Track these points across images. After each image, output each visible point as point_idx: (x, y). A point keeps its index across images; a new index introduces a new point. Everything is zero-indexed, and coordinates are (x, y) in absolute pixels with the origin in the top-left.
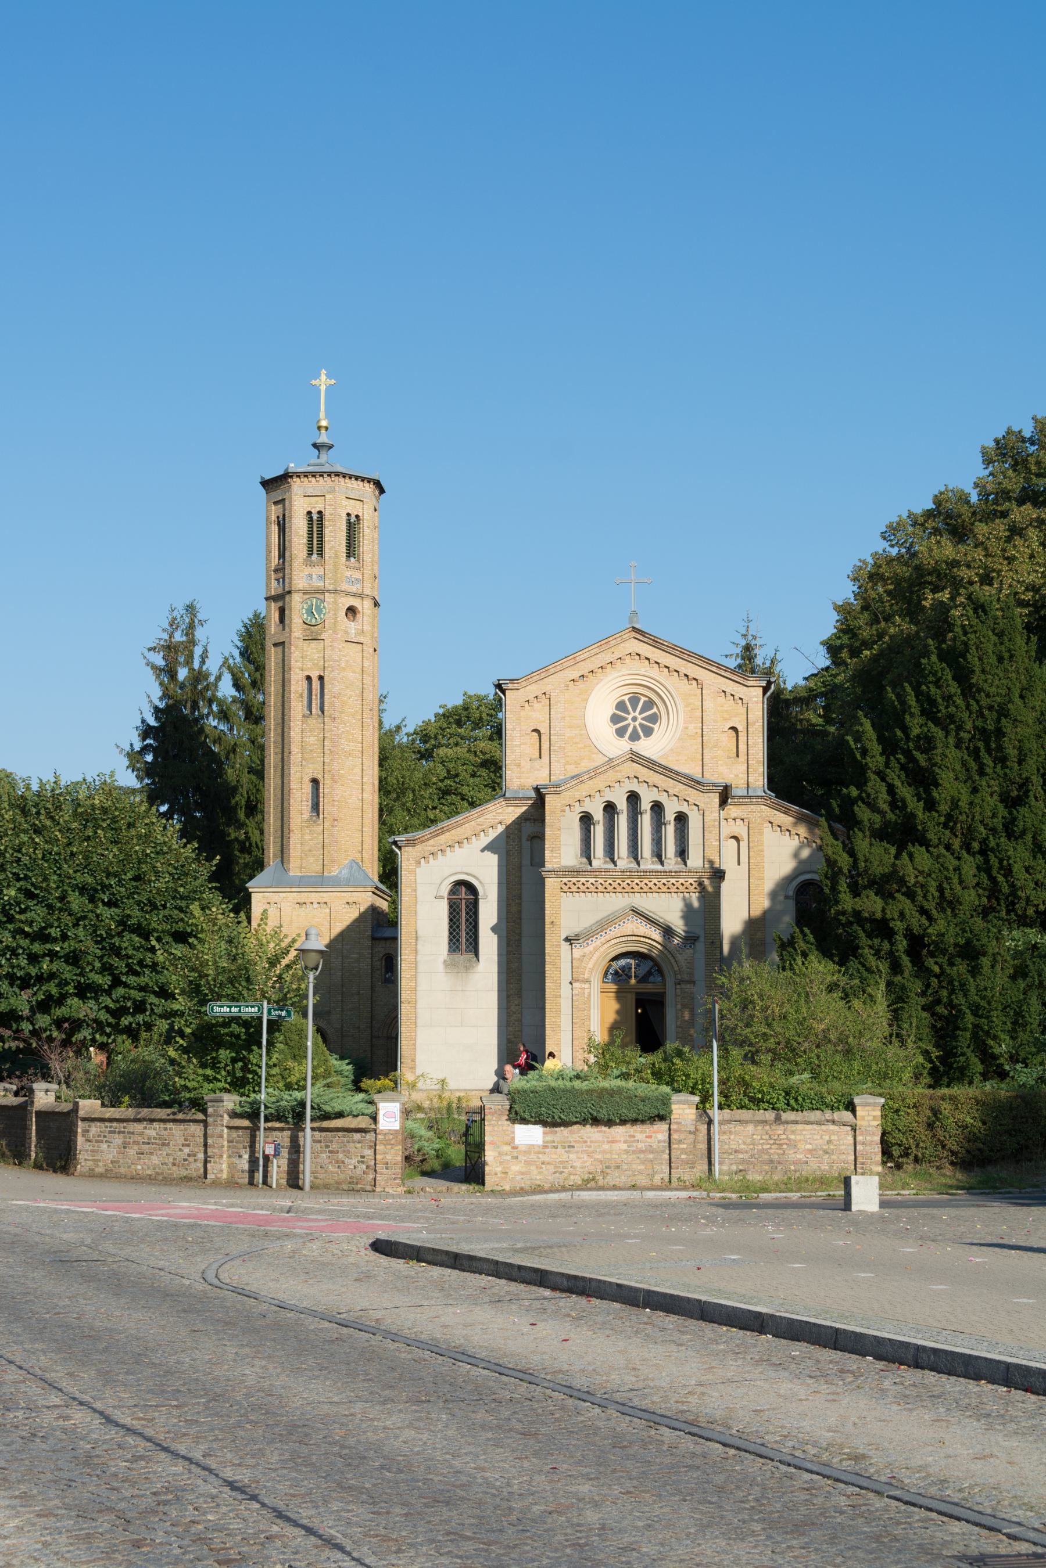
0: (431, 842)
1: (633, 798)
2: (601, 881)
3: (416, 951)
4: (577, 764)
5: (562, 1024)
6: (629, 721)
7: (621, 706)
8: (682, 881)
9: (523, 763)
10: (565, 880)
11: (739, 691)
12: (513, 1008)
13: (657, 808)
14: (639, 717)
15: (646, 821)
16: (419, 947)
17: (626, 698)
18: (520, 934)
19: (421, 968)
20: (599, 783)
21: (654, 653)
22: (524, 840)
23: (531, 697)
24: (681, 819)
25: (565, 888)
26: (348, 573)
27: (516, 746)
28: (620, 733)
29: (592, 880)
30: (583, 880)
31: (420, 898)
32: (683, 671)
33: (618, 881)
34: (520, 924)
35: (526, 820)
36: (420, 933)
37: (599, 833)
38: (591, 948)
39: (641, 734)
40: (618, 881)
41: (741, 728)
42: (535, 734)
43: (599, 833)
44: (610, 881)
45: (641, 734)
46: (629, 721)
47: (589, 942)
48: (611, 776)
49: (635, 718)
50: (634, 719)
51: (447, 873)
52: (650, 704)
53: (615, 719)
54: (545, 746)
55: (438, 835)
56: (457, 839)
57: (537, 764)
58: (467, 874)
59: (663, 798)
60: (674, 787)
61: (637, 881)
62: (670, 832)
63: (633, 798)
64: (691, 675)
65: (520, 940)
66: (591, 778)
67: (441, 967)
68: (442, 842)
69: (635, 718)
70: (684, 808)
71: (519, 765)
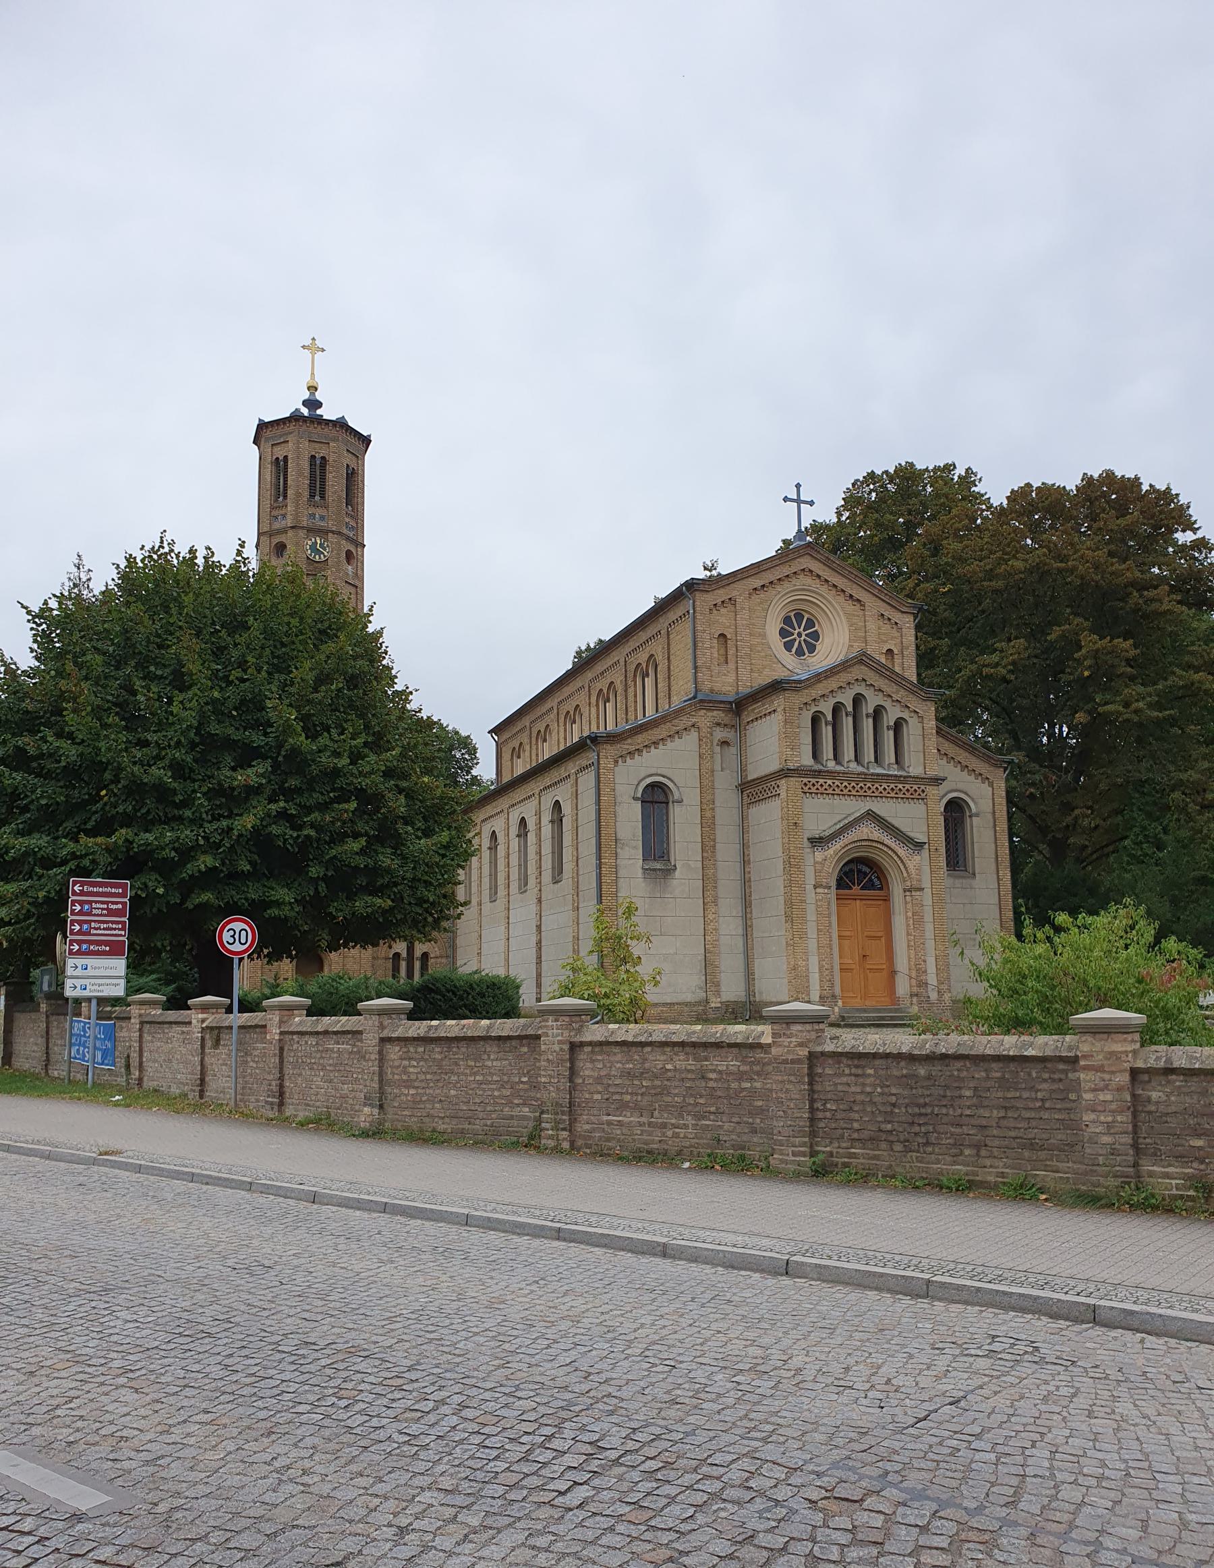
0: (629, 741)
1: (858, 700)
2: (837, 783)
3: (616, 854)
4: (760, 672)
5: (809, 931)
6: (795, 636)
7: (787, 620)
8: (907, 786)
9: (713, 668)
10: (805, 780)
11: (896, 617)
12: (711, 917)
13: (878, 713)
14: (804, 634)
15: (868, 725)
16: (619, 850)
17: (792, 614)
18: (714, 840)
19: (621, 873)
20: (833, 683)
21: (824, 571)
22: (715, 744)
23: (719, 601)
24: (898, 726)
25: (806, 789)
26: (347, 520)
27: (706, 648)
28: (788, 646)
29: (829, 782)
30: (822, 781)
31: (619, 799)
32: (849, 591)
33: (853, 784)
34: (714, 829)
35: (718, 724)
36: (619, 836)
37: (827, 732)
38: (831, 851)
39: (794, 650)
40: (853, 784)
41: (896, 651)
42: (721, 639)
43: (827, 732)
44: (845, 783)
45: (794, 650)
46: (795, 636)
47: (830, 845)
48: (844, 677)
49: (799, 633)
50: (800, 635)
51: (643, 775)
52: (810, 623)
53: (783, 633)
54: (731, 652)
55: (636, 734)
56: (654, 739)
57: (724, 668)
58: (664, 776)
59: (887, 704)
60: (897, 692)
61: (869, 785)
62: (889, 737)
63: (858, 700)
64: (856, 596)
65: (714, 847)
66: (827, 677)
67: (640, 873)
68: (639, 741)
69: (799, 633)
70: (906, 715)
71: (709, 668)
